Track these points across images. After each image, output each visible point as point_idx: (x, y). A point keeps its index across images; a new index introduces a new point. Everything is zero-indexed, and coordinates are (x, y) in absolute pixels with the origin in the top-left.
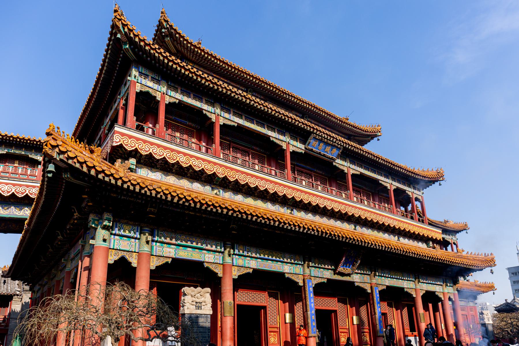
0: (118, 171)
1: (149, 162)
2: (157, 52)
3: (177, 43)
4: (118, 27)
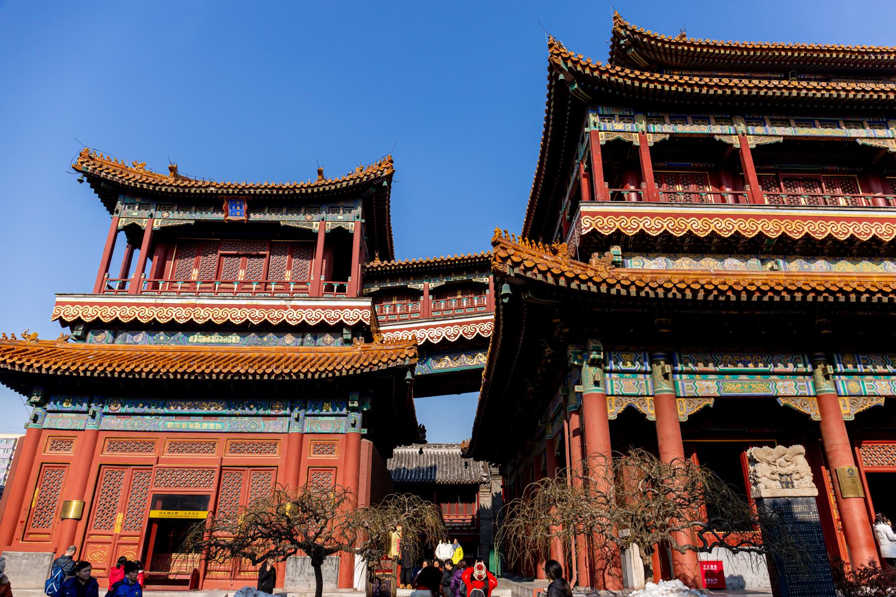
0: (597, 271)
1: (642, 245)
2: (620, 76)
3: (648, 51)
4: (558, 66)
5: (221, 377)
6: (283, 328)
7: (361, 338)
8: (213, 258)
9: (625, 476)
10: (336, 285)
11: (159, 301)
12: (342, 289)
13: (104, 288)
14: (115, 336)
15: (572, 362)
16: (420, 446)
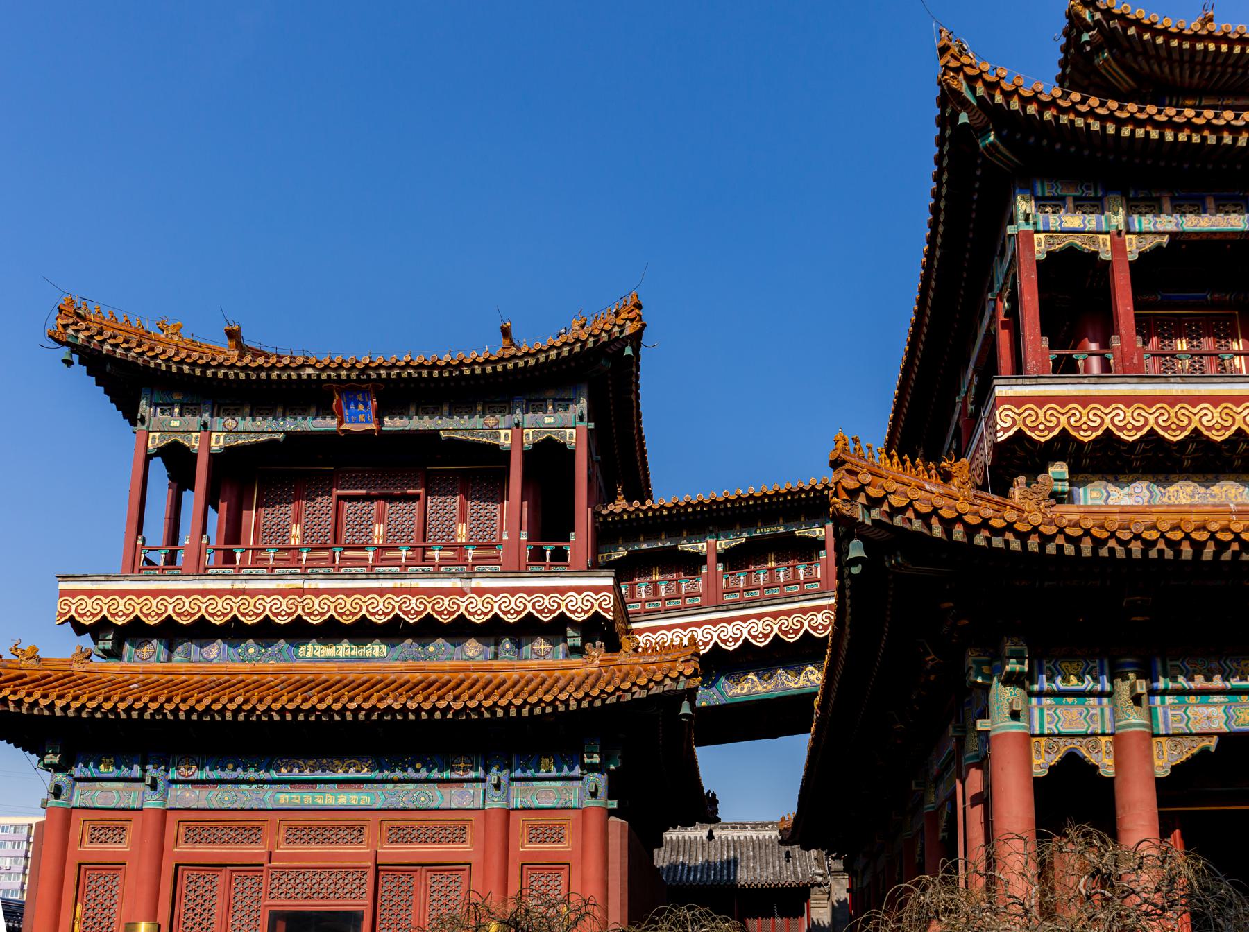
0: (1022, 511)
1: (1108, 458)
5: (362, 716)
6: (460, 629)
7: (598, 643)
8: (325, 504)
9: (1057, 870)
10: (549, 549)
11: (239, 585)
12: (559, 556)
13: (139, 565)
14: (171, 649)
15: (972, 678)
16: (708, 827)
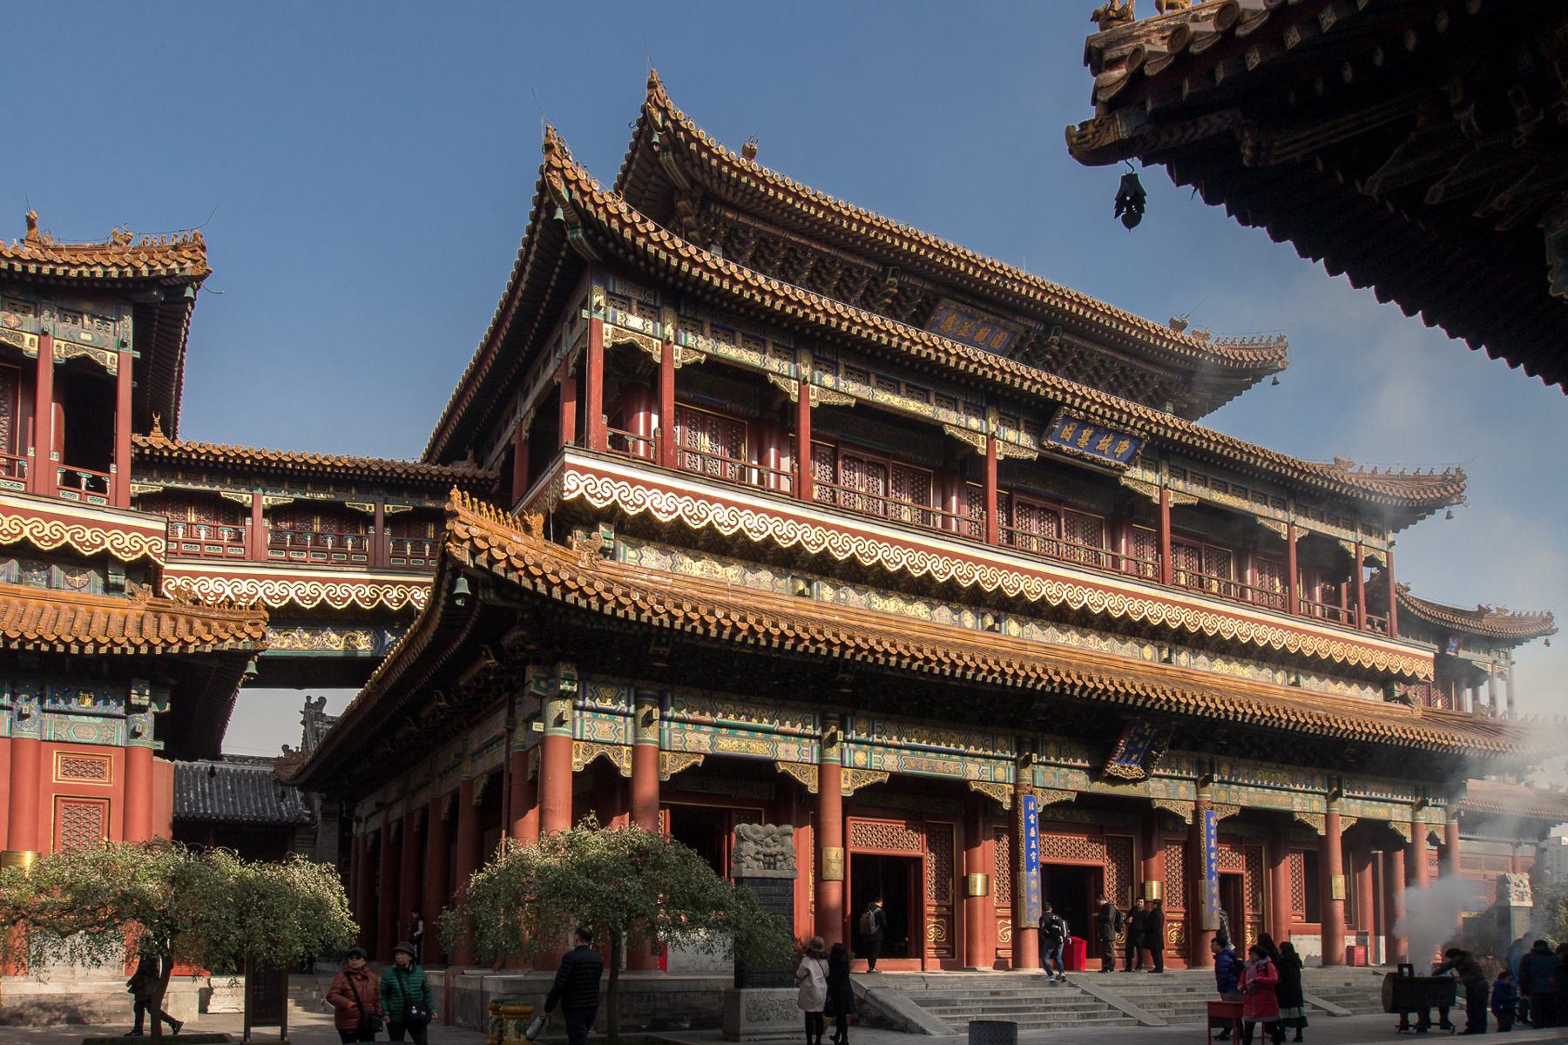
7: (145, 586)
